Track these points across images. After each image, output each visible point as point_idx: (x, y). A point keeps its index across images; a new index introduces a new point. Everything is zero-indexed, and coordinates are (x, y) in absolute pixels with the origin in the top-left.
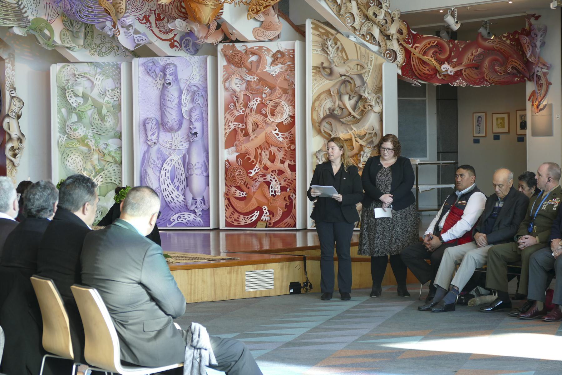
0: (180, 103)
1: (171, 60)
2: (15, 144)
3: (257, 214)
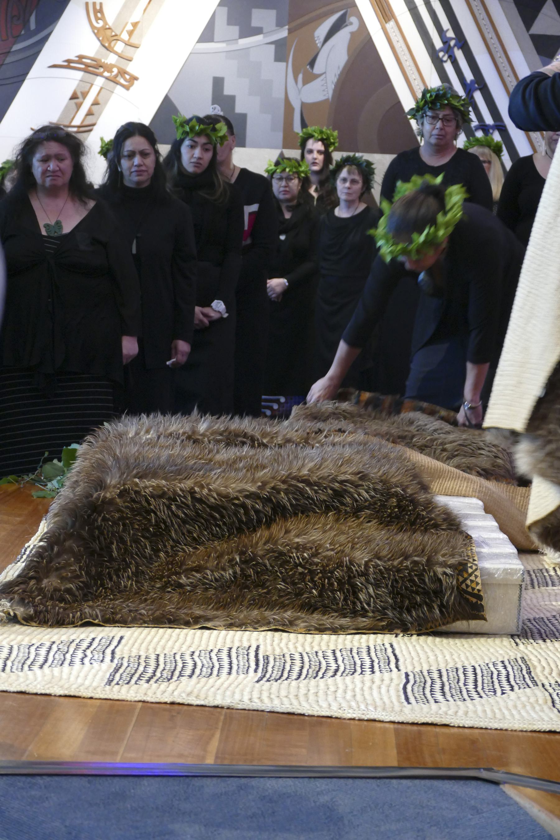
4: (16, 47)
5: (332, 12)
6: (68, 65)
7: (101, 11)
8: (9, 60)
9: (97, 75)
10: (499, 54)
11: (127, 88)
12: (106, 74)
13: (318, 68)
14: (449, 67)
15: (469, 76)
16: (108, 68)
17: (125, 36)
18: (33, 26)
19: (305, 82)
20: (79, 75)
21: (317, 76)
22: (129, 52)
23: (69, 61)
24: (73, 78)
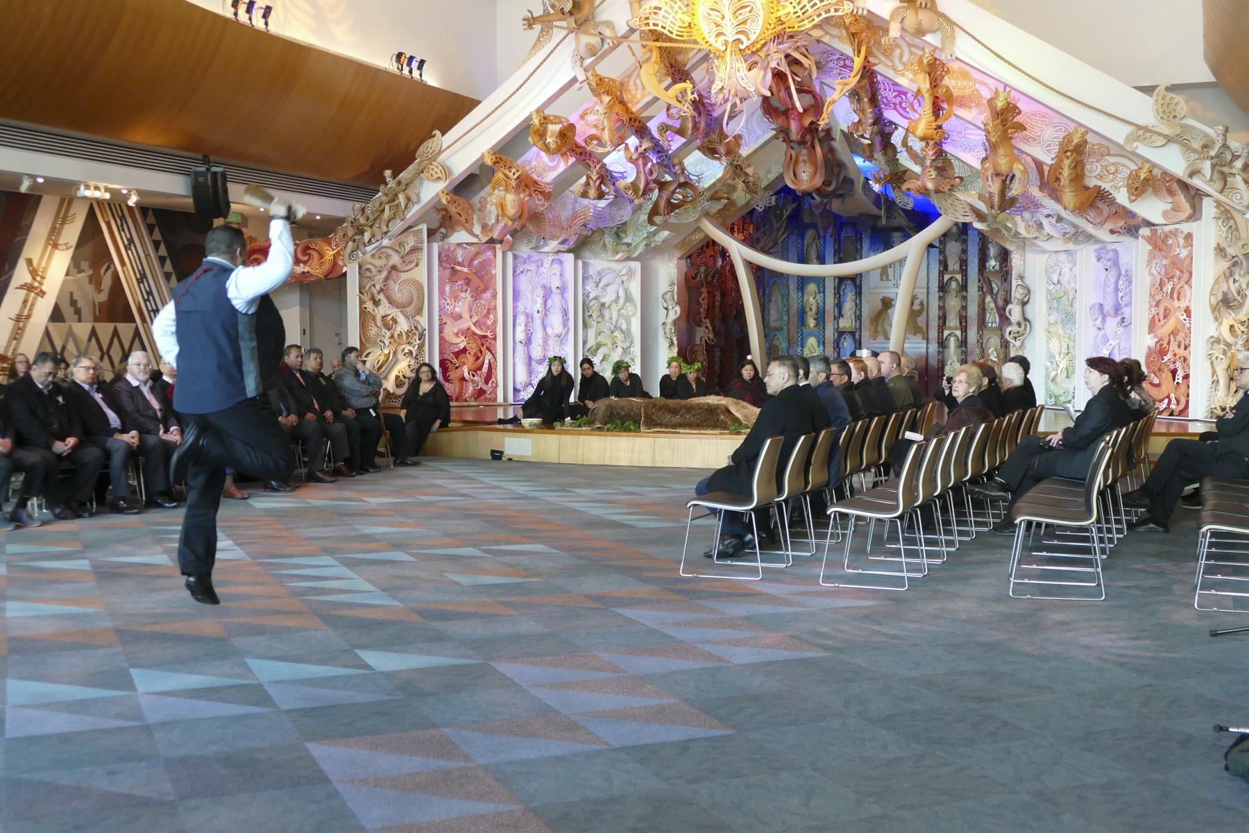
0: (1117, 289)
1: (1115, 246)
2: (1014, 328)
3: (1166, 401)
6: (21, 287)
20: (25, 292)
24: (23, 293)
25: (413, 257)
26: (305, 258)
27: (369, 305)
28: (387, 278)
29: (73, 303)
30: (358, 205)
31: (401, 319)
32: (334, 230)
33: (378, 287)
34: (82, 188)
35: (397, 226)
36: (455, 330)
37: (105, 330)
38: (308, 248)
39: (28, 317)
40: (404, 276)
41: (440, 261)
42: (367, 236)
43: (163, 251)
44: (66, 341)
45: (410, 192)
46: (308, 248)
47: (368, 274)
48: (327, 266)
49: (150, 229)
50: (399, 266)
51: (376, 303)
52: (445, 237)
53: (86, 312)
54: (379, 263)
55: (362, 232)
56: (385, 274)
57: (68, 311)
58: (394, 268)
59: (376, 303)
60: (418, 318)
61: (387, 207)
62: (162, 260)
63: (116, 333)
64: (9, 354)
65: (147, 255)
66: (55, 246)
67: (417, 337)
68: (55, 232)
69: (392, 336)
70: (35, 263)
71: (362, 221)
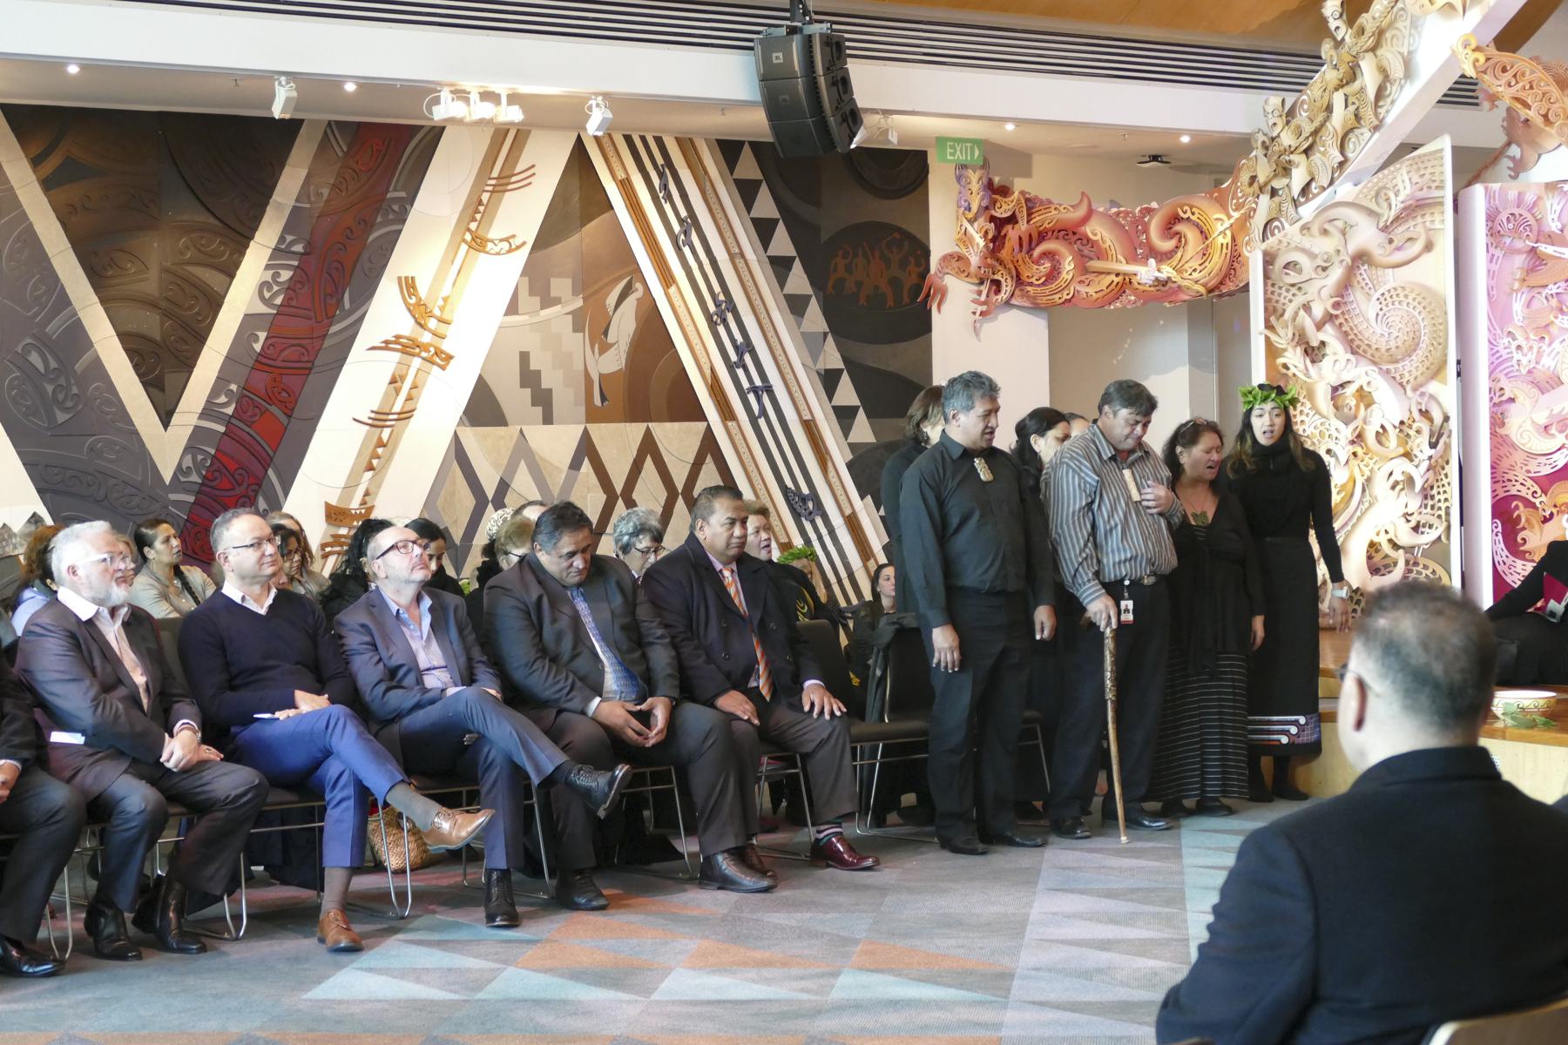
4: (334, 329)
5: (620, 279)
6: (386, 346)
7: (414, 287)
8: (327, 344)
9: (413, 355)
10: (763, 315)
11: (443, 368)
12: (424, 354)
13: (611, 338)
14: (721, 329)
15: (739, 338)
16: (425, 347)
17: (437, 312)
18: (347, 305)
19: (602, 352)
20: (396, 356)
21: (612, 345)
22: (442, 328)
23: (387, 342)
25: (1417, 227)
26: (1168, 245)
27: (1293, 358)
28: (1345, 285)
29: (529, 378)
30: (1274, 100)
31: (1382, 391)
32: (1230, 170)
33: (1318, 311)
34: (445, 95)
35: (1368, 148)
36: (1542, 420)
37: (618, 442)
38: (1176, 219)
39: (405, 415)
40: (1391, 279)
41: (1494, 233)
42: (1298, 178)
43: (782, 243)
44: (511, 468)
45: (1390, 55)
46: (1176, 219)
47: (1293, 277)
48: (1217, 261)
49: (747, 192)
50: (1378, 253)
51: (1314, 353)
52: (1519, 168)
53: (566, 398)
54: (1324, 246)
55: (1285, 170)
56: (1337, 273)
57: (512, 396)
58: (1361, 258)
59: (1314, 353)
60: (1433, 387)
61: (1338, 99)
62: (780, 266)
63: (649, 447)
64: (355, 504)
65: (736, 256)
66: (479, 243)
67: (1424, 440)
68: (477, 210)
69: (1359, 438)
70: (422, 290)
71: (1287, 139)
